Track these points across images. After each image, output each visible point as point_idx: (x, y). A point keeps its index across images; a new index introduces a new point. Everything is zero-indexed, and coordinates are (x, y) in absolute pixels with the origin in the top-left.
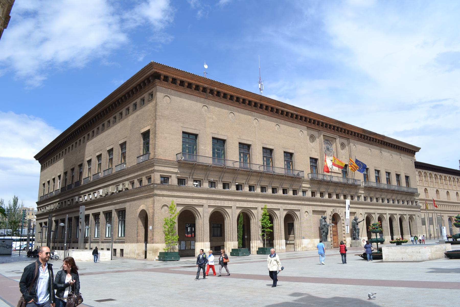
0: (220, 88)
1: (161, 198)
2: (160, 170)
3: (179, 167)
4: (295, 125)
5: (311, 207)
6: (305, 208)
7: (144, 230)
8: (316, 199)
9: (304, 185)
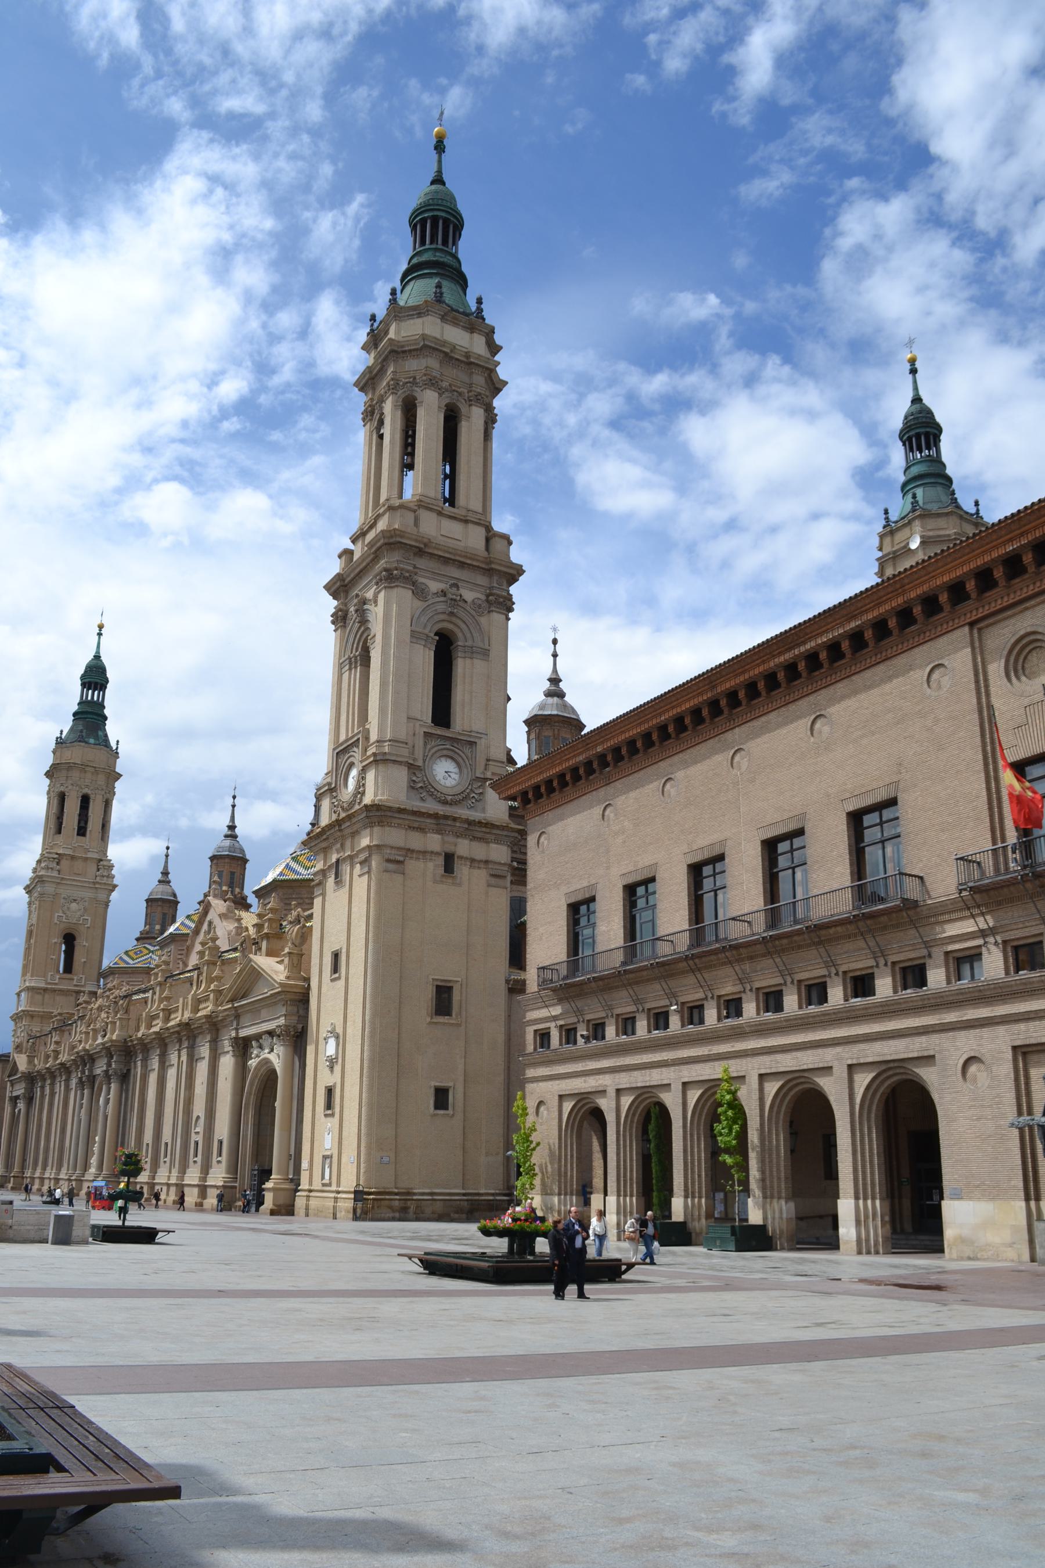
0: (607, 740)
1: (535, 1085)
2: (536, 1020)
3: (560, 1001)
4: (901, 661)
5: (1001, 1030)
6: (957, 1047)
7: (602, 1161)
8: (939, 995)
9: (953, 929)
